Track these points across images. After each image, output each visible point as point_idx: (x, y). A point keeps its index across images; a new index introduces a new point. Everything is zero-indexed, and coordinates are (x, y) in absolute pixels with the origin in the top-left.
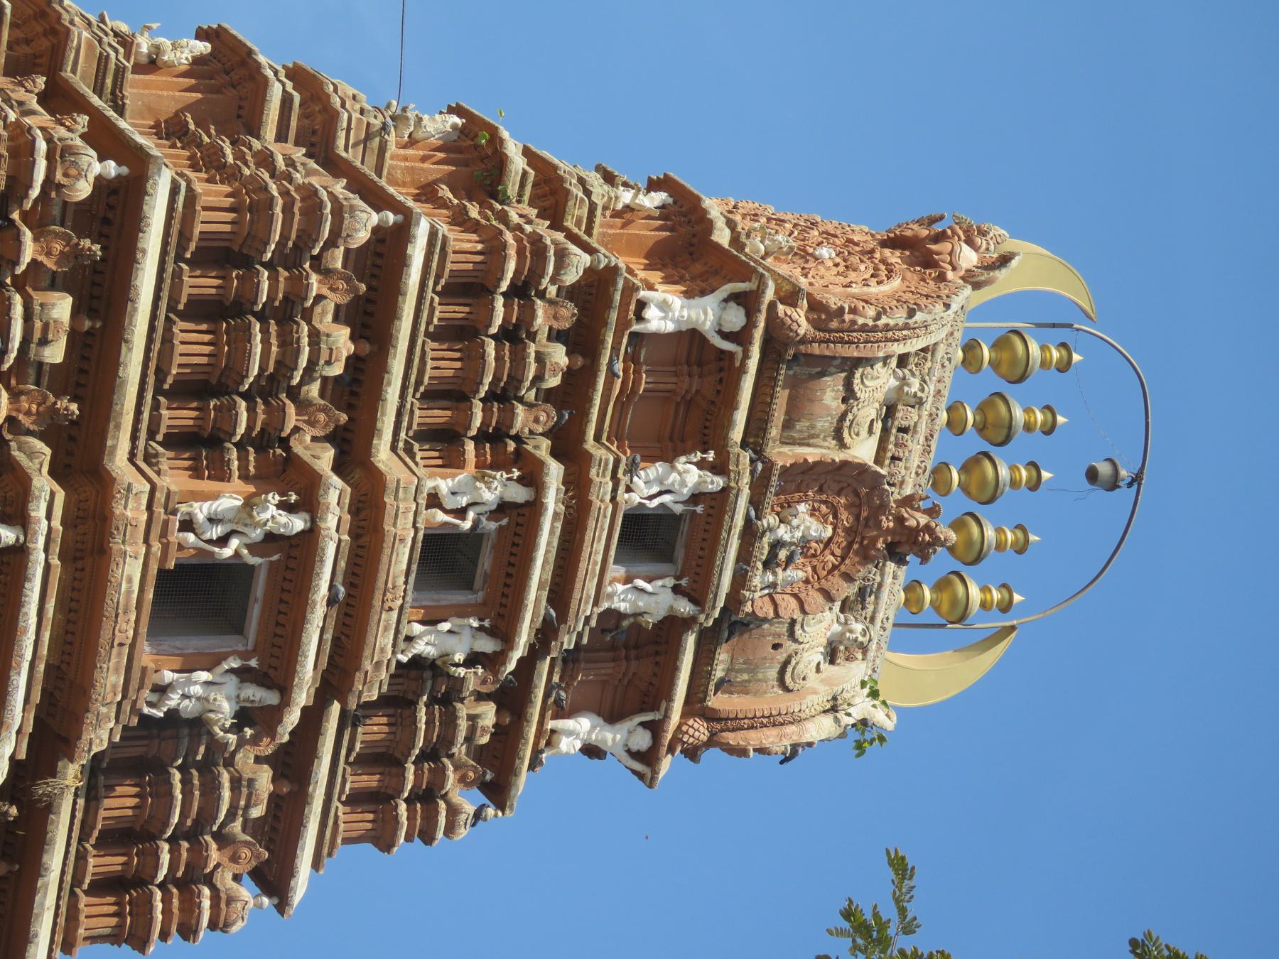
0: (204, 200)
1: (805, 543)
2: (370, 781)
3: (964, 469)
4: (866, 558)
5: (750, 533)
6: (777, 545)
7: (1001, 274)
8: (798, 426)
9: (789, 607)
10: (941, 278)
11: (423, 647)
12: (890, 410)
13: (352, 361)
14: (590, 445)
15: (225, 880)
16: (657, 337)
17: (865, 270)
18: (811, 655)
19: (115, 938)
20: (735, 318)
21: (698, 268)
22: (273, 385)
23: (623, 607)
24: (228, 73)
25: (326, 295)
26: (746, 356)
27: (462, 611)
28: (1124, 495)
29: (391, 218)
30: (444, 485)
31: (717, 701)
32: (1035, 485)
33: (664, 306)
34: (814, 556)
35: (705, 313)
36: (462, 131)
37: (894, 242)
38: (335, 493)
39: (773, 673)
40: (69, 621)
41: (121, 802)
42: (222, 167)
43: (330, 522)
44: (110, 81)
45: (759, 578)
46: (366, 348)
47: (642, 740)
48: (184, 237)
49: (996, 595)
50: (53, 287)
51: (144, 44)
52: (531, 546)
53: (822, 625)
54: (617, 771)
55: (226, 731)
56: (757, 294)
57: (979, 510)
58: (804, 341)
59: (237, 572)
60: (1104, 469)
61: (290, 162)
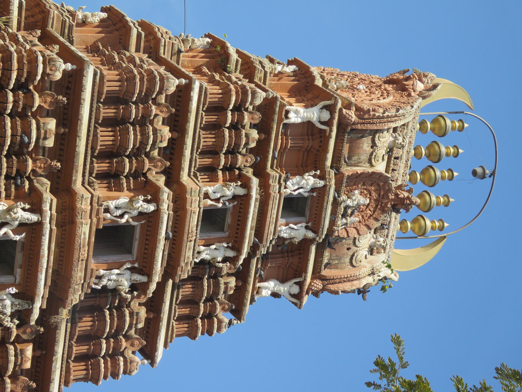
0: (107, 78)
1: (358, 205)
2: (186, 311)
3: (422, 173)
4: (383, 211)
5: (336, 203)
6: (347, 208)
7: (434, 93)
8: (354, 158)
9: (353, 233)
10: (409, 95)
11: (205, 255)
12: (390, 151)
13: (171, 141)
14: (269, 170)
15: (129, 354)
16: (294, 125)
17: (378, 93)
18: (363, 252)
19: (85, 379)
20: (326, 115)
21: (310, 96)
22: (139, 152)
24: (115, 25)
25: (159, 114)
26: (331, 131)
27: (220, 240)
28: (488, 180)
29: (184, 81)
30: (210, 189)
31: (325, 272)
32: (451, 178)
33: (297, 112)
34: (362, 211)
35: (314, 114)
36: (211, 45)
37: (389, 82)
38: (166, 194)
39: (347, 260)
40: (61, 252)
41: (85, 324)
42: (114, 64)
43: (165, 206)
44: (67, 31)
45: (340, 222)
46: (176, 135)
47: (296, 290)
48: (100, 93)
49: (437, 224)
50: (48, 116)
51: (80, 15)
52: (247, 213)
53: (367, 239)
54: (286, 302)
55: (126, 293)
56: (334, 105)
57: (429, 189)
58: (354, 124)
59: (128, 228)
60: (479, 170)
61: (142, 60)
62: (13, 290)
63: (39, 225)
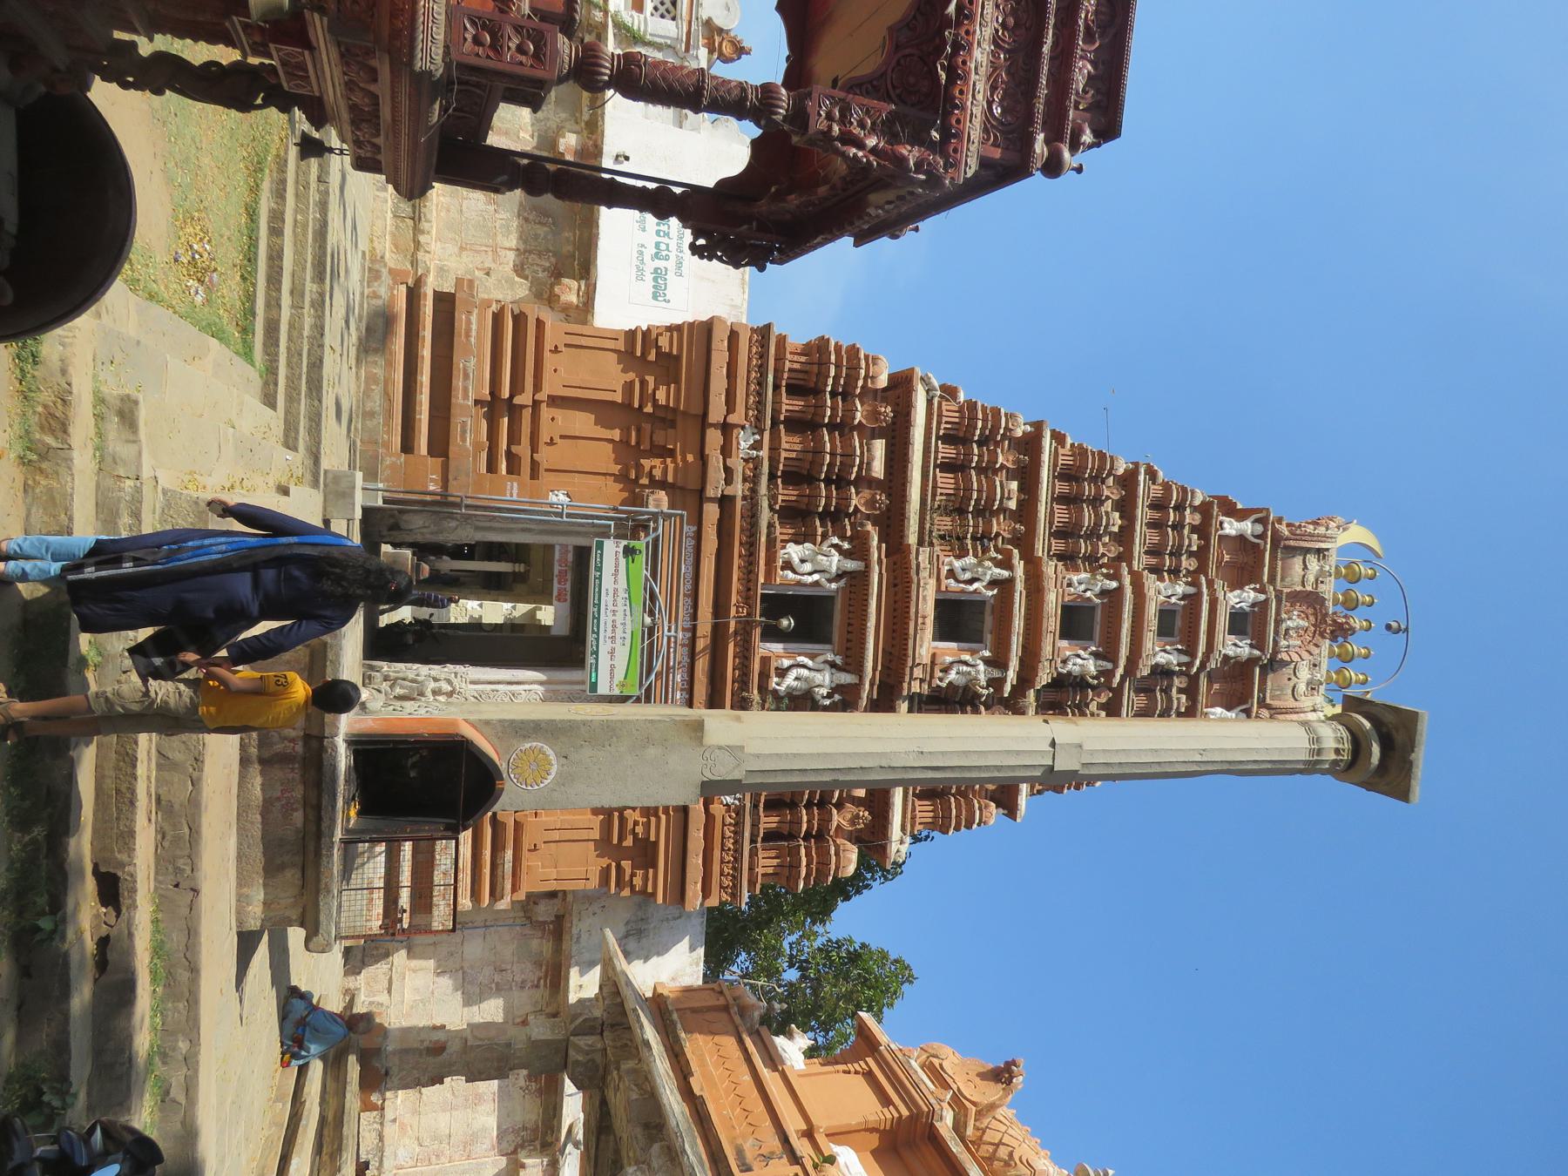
1: (1297, 629)
5: (1278, 622)
9: (1295, 658)
11: (1162, 658)
16: (1227, 536)
20: (1259, 528)
23: (1231, 653)
28: (1402, 636)
35: (1247, 527)
45: (1283, 643)
56: (1267, 517)
60: (1394, 625)
62: (987, 654)
63: (1010, 581)
